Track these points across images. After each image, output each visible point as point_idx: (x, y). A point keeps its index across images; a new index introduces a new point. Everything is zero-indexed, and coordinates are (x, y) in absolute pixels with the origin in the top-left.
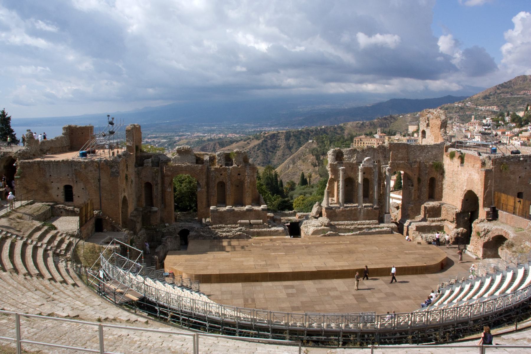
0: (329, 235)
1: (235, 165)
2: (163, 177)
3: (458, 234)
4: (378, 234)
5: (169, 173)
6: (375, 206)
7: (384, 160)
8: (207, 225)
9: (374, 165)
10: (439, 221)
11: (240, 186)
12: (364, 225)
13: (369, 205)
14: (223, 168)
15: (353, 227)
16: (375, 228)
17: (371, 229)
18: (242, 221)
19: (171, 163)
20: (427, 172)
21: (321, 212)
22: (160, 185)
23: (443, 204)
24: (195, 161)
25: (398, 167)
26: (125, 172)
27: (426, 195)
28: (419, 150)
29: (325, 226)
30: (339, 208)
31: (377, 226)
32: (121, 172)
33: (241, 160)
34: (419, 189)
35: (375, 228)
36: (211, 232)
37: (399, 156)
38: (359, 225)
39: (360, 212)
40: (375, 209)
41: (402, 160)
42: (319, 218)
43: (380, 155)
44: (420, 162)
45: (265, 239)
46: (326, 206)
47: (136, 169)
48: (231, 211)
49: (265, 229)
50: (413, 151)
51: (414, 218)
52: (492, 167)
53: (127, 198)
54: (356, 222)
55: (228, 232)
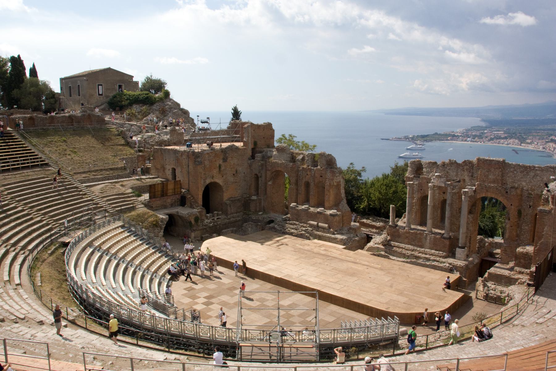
0: (378, 255)
1: (319, 167)
2: (266, 170)
4: (432, 268)
5: (270, 169)
6: (445, 235)
7: (470, 180)
8: (286, 220)
9: (445, 184)
11: (321, 188)
12: (426, 254)
13: (443, 232)
14: (309, 169)
15: (410, 253)
16: (434, 260)
17: (428, 260)
19: (272, 160)
20: (531, 204)
22: (263, 178)
24: (289, 159)
25: (487, 191)
26: (221, 162)
30: (404, 228)
31: (438, 259)
32: (207, 163)
33: (324, 162)
34: (519, 226)
35: (434, 260)
36: (283, 227)
37: (490, 177)
38: (420, 253)
40: (445, 238)
41: (494, 182)
43: (466, 173)
44: (522, 189)
45: (335, 247)
47: (249, 162)
48: (306, 211)
49: (328, 235)
50: (513, 172)
51: (508, 264)
52: (552, 207)
53: (221, 184)
54: (419, 249)
55: (296, 230)
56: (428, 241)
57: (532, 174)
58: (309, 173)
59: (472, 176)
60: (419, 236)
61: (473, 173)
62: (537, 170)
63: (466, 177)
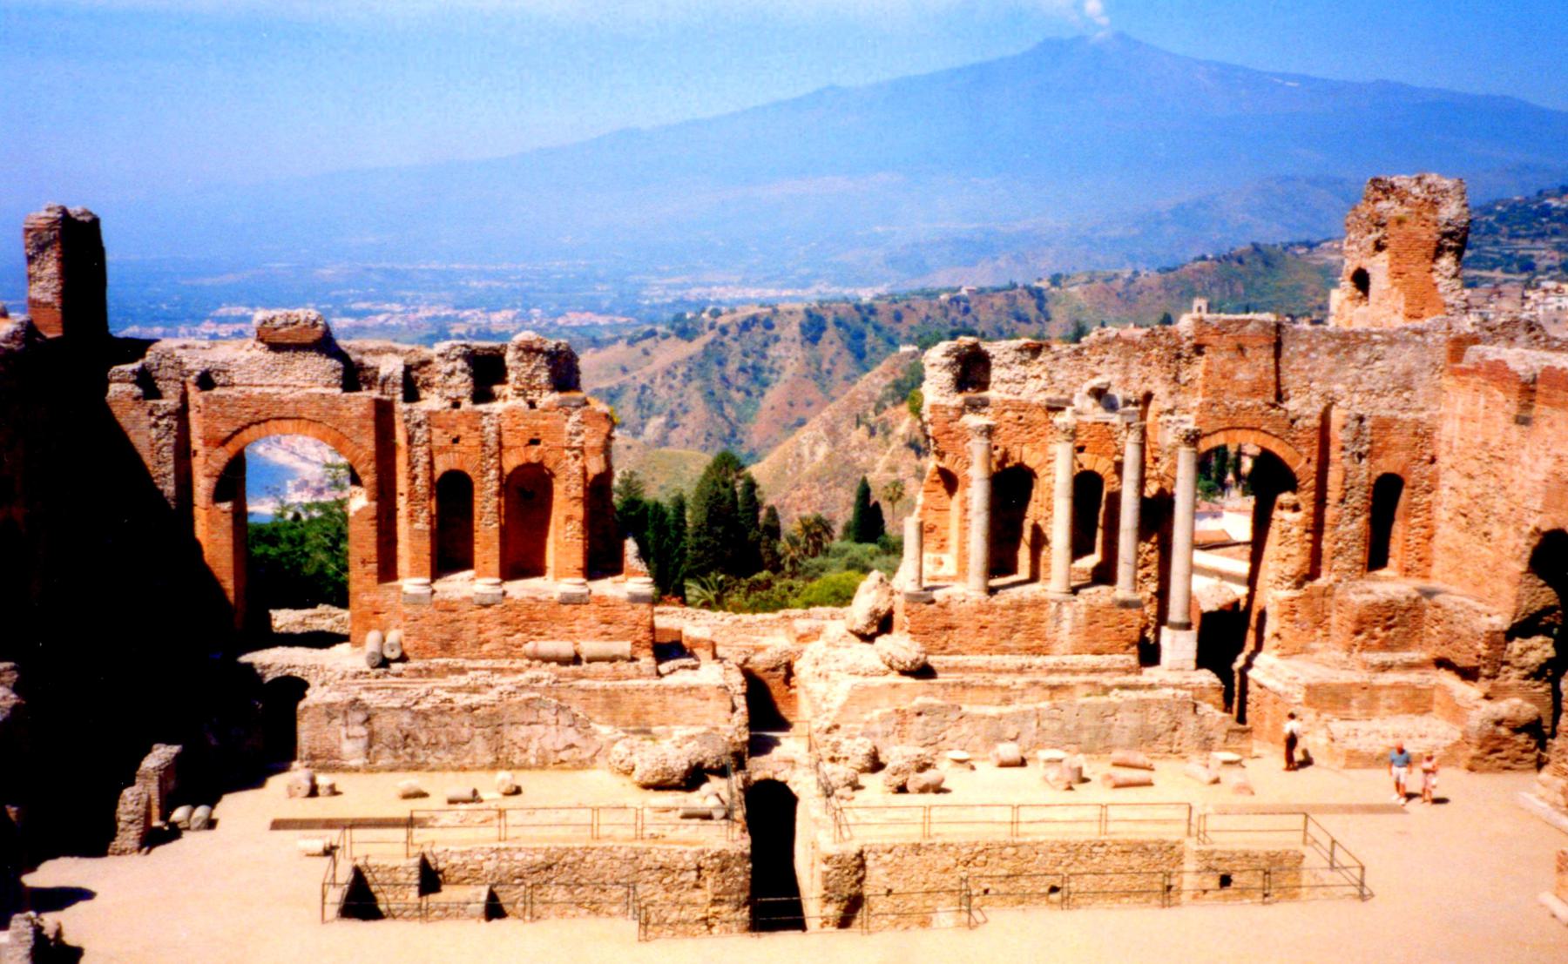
3: (1499, 723)
10: (1410, 666)
12: (1074, 672)
14: (465, 415)
18: (547, 646)
21: (890, 613)
23: (1429, 594)
27: (1358, 553)
28: (1332, 352)
29: (903, 673)
37: (1240, 376)
38: (1051, 671)
39: (1058, 619)
40: (1125, 604)
41: (1254, 392)
42: (880, 641)
46: (911, 588)
50: (1305, 355)
54: (1038, 661)
56: (1067, 625)
57: (1362, 355)
58: (462, 430)
59: (1176, 379)
60: (1029, 614)
61: (1178, 369)
62: (1376, 343)
63: (1158, 382)
